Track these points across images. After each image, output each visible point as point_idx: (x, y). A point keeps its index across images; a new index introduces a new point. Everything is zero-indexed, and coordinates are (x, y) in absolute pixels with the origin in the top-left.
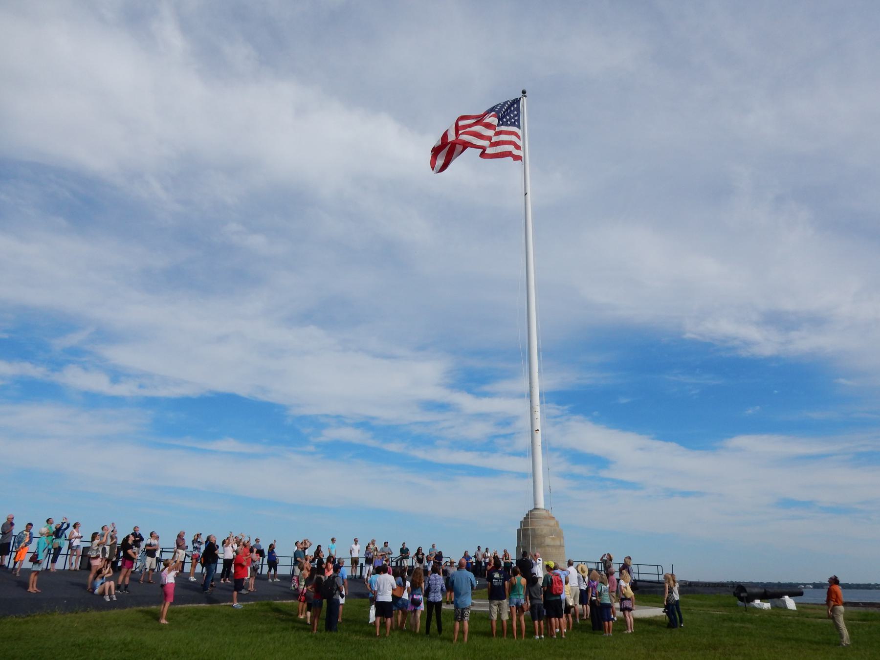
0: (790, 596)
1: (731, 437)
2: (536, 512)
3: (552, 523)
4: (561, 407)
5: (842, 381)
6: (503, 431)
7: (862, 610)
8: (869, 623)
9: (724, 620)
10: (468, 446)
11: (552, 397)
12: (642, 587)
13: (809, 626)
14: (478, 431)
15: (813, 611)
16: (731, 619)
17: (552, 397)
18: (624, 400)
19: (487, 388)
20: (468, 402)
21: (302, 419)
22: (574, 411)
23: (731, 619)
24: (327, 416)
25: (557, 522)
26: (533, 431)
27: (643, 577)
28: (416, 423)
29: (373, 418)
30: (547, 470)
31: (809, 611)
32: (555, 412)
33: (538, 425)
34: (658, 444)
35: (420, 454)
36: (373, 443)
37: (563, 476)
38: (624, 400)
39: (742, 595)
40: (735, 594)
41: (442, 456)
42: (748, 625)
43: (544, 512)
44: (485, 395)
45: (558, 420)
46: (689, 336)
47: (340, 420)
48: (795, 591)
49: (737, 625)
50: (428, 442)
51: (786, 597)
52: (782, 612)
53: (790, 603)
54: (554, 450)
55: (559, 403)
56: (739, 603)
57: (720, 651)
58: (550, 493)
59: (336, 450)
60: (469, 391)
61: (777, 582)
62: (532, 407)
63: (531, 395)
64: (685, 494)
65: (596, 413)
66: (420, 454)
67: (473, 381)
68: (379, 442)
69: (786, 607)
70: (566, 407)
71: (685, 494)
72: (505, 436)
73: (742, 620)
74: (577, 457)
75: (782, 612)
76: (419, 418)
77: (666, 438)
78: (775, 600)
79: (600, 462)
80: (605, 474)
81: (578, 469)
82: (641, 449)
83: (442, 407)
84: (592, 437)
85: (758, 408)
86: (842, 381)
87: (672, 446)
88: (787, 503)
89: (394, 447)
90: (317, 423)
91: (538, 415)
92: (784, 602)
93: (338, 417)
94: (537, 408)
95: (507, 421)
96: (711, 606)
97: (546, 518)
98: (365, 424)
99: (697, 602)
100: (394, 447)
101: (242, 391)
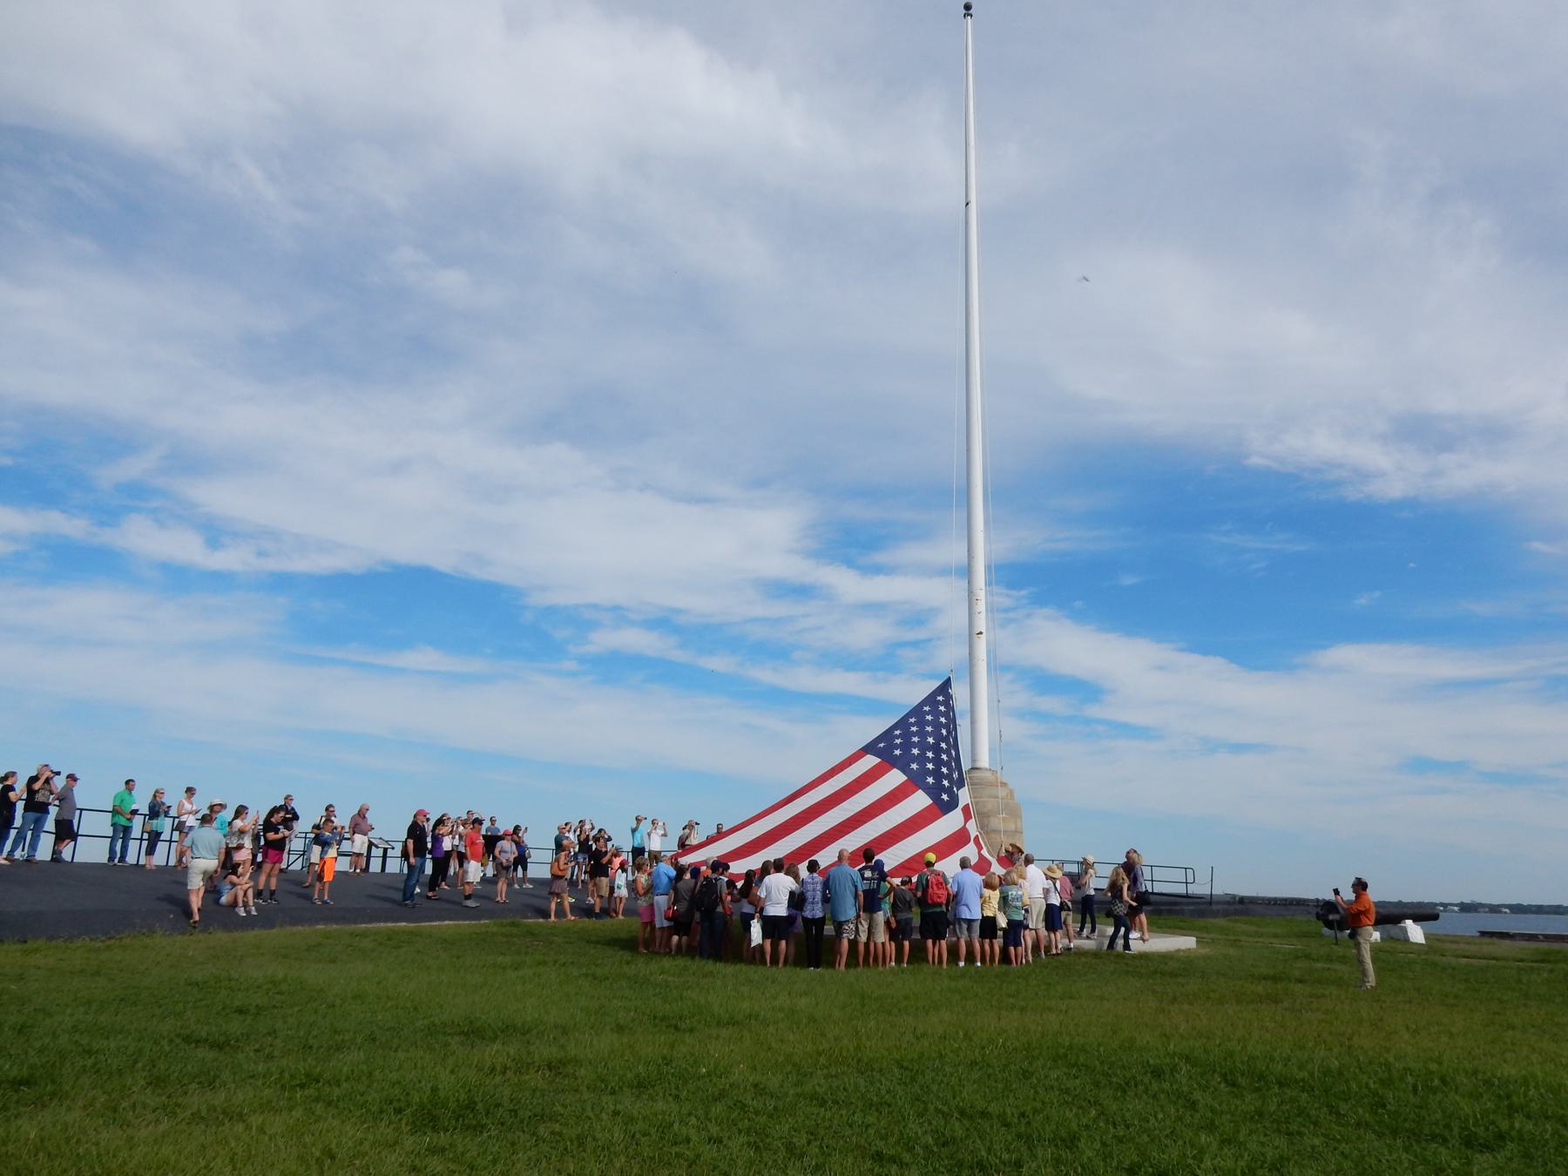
0: (1416, 919)
1: (1325, 648)
2: (976, 774)
3: (1001, 792)
4: (1014, 593)
5: (1538, 546)
6: (912, 636)
7: (1544, 946)
8: (1550, 966)
9: (1297, 957)
10: (849, 661)
11: (1008, 575)
12: (1156, 903)
13: (1444, 969)
14: (867, 634)
15: (1454, 946)
16: (1308, 957)
17: (1008, 575)
18: (1128, 580)
19: (880, 558)
20: (847, 584)
21: (551, 610)
22: (1039, 601)
23: (1308, 957)
24: (595, 606)
25: (1012, 792)
26: (972, 635)
27: (1158, 888)
28: (755, 620)
29: (679, 611)
30: (995, 703)
31: (1447, 946)
32: (1007, 602)
33: (981, 624)
34: (1193, 659)
35: (766, 675)
36: (680, 656)
37: (1022, 714)
38: (1128, 580)
39: (1331, 917)
40: (1318, 917)
41: (805, 679)
42: (1336, 966)
43: (988, 774)
44: (878, 570)
45: (1011, 615)
46: (1255, 461)
47: (619, 615)
48: (1425, 914)
49: (1319, 965)
50: (778, 653)
51: (1409, 922)
52: (1400, 947)
53: (1415, 932)
54: (1007, 668)
55: (1011, 585)
56: (1326, 930)
57: (1286, 1004)
58: (1000, 745)
59: (615, 669)
60: (850, 563)
61: (1394, 899)
62: (971, 593)
63: (967, 572)
64: (1238, 748)
65: (1079, 604)
66: (766, 675)
67: (853, 544)
68: (689, 653)
69: (1407, 940)
70: (1023, 593)
71: (1238, 748)
72: (915, 644)
73: (1329, 959)
74: (1045, 682)
75: (1400, 947)
76: (759, 611)
77: (1205, 650)
78: (1389, 927)
79: (1085, 690)
80: (1093, 711)
81: (1049, 703)
82: (1161, 668)
83: (801, 591)
84: (1072, 646)
85: (1377, 594)
86: (1538, 546)
87: (1215, 663)
88: (1421, 765)
89: (718, 663)
90: (581, 620)
91: (981, 606)
92: (1405, 930)
93: (616, 609)
94: (981, 594)
95: (917, 617)
96: (1276, 936)
97: (992, 785)
98: (662, 622)
99: (1254, 928)
100: (718, 663)
101: (443, 562)
